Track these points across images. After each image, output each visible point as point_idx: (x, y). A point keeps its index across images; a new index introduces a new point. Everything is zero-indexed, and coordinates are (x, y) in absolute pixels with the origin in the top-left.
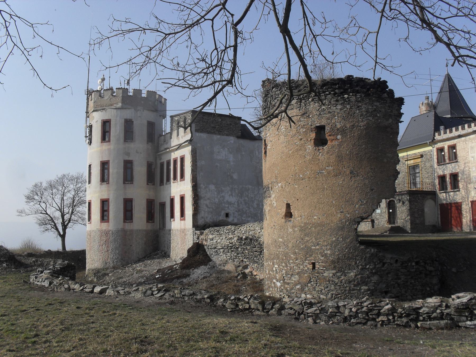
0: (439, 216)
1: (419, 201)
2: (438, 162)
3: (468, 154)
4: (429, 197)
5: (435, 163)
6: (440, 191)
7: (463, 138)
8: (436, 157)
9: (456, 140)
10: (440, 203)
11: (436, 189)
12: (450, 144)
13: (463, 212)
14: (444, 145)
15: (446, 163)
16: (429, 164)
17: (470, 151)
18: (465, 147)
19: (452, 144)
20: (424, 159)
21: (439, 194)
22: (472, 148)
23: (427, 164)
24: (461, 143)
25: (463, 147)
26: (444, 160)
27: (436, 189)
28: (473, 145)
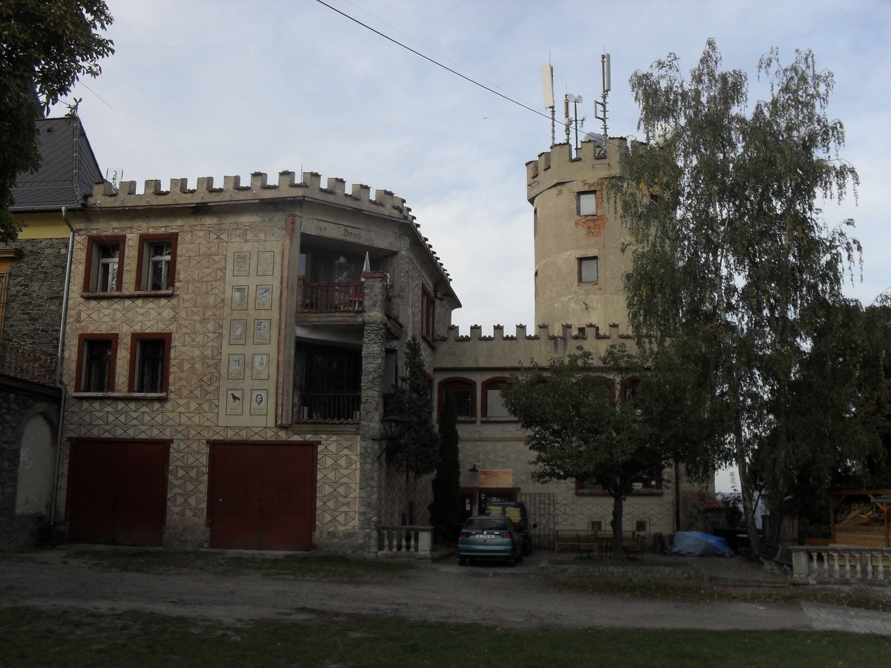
0: (64, 482)
1: (8, 418)
2: (86, 287)
3: (220, 274)
4: (41, 406)
5: (72, 288)
6: (77, 389)
7: (209, 221)
8: (82, 268)
9: (179, 222)
10: (71, 434)
11: (61, 383)
12: (151, 231)
13: (170, 477)
14: (123, 229)
15: (125, 292)
16: (45, 289)
17: (230, 267)
18: (214, 250)
19: (162, 231)
20: (26, 269)
21: (73, 401)
22: (241, 258)
23: (35, 286)
24: (201, 234)
25: (203, 250)
26: (105, 287)
27: (65, 380)
28: (247, 247)
